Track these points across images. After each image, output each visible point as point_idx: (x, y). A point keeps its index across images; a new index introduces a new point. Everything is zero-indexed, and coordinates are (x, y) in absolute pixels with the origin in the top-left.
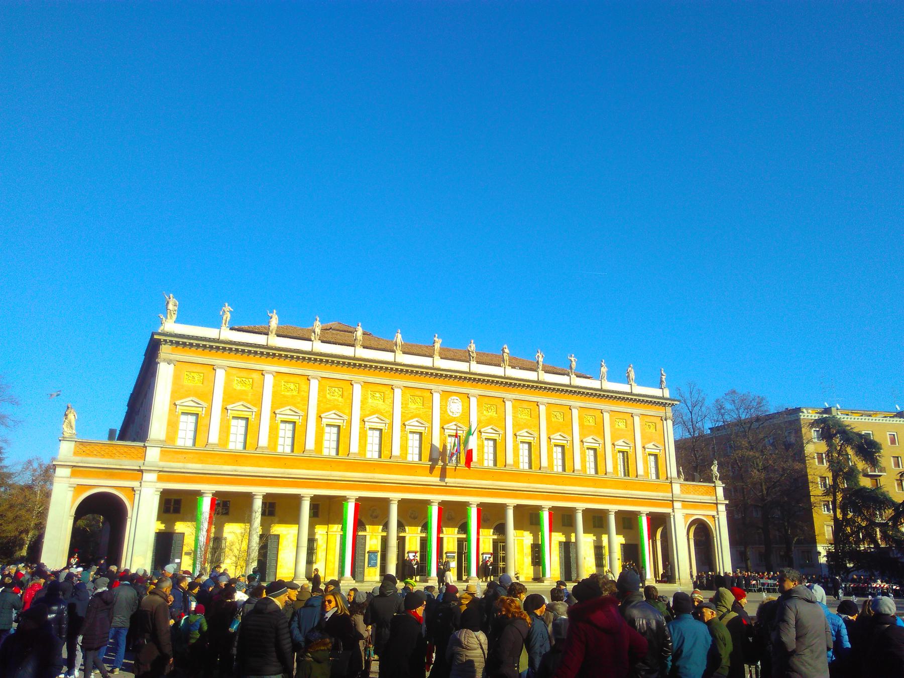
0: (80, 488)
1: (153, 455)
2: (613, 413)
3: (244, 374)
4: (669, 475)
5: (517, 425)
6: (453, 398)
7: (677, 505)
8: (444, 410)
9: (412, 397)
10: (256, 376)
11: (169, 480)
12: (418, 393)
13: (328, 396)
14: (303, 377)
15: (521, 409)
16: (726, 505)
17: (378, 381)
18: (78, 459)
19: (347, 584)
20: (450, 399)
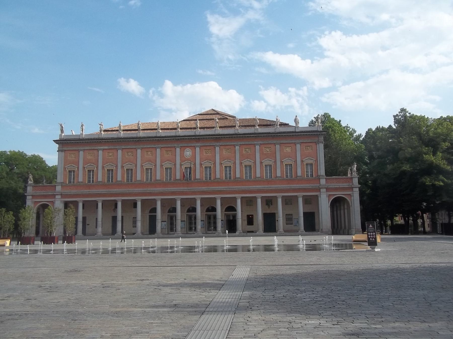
0: (36, 203)
1: (59, 188)
2: (281, 144)
3: (91, 152)
4: (319, 174)
5: (222, 159)
6: (186, 149)
7: (323, 190)
8: (182, 155)
9: (166, 152)
10: (95, 152)
11: (65, 198)
12: (169, 149)
13: (127, 156)
14: (114, 150)
15: (225, 150)
16: (359, 187)
17: (148, 146)
18: (34, 192)
19: (137, 236)
20: (185, 150)
